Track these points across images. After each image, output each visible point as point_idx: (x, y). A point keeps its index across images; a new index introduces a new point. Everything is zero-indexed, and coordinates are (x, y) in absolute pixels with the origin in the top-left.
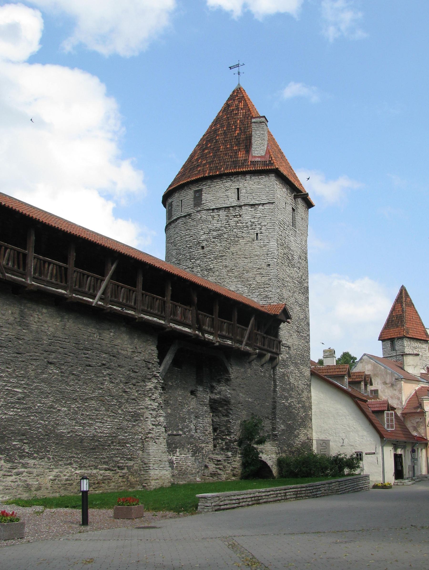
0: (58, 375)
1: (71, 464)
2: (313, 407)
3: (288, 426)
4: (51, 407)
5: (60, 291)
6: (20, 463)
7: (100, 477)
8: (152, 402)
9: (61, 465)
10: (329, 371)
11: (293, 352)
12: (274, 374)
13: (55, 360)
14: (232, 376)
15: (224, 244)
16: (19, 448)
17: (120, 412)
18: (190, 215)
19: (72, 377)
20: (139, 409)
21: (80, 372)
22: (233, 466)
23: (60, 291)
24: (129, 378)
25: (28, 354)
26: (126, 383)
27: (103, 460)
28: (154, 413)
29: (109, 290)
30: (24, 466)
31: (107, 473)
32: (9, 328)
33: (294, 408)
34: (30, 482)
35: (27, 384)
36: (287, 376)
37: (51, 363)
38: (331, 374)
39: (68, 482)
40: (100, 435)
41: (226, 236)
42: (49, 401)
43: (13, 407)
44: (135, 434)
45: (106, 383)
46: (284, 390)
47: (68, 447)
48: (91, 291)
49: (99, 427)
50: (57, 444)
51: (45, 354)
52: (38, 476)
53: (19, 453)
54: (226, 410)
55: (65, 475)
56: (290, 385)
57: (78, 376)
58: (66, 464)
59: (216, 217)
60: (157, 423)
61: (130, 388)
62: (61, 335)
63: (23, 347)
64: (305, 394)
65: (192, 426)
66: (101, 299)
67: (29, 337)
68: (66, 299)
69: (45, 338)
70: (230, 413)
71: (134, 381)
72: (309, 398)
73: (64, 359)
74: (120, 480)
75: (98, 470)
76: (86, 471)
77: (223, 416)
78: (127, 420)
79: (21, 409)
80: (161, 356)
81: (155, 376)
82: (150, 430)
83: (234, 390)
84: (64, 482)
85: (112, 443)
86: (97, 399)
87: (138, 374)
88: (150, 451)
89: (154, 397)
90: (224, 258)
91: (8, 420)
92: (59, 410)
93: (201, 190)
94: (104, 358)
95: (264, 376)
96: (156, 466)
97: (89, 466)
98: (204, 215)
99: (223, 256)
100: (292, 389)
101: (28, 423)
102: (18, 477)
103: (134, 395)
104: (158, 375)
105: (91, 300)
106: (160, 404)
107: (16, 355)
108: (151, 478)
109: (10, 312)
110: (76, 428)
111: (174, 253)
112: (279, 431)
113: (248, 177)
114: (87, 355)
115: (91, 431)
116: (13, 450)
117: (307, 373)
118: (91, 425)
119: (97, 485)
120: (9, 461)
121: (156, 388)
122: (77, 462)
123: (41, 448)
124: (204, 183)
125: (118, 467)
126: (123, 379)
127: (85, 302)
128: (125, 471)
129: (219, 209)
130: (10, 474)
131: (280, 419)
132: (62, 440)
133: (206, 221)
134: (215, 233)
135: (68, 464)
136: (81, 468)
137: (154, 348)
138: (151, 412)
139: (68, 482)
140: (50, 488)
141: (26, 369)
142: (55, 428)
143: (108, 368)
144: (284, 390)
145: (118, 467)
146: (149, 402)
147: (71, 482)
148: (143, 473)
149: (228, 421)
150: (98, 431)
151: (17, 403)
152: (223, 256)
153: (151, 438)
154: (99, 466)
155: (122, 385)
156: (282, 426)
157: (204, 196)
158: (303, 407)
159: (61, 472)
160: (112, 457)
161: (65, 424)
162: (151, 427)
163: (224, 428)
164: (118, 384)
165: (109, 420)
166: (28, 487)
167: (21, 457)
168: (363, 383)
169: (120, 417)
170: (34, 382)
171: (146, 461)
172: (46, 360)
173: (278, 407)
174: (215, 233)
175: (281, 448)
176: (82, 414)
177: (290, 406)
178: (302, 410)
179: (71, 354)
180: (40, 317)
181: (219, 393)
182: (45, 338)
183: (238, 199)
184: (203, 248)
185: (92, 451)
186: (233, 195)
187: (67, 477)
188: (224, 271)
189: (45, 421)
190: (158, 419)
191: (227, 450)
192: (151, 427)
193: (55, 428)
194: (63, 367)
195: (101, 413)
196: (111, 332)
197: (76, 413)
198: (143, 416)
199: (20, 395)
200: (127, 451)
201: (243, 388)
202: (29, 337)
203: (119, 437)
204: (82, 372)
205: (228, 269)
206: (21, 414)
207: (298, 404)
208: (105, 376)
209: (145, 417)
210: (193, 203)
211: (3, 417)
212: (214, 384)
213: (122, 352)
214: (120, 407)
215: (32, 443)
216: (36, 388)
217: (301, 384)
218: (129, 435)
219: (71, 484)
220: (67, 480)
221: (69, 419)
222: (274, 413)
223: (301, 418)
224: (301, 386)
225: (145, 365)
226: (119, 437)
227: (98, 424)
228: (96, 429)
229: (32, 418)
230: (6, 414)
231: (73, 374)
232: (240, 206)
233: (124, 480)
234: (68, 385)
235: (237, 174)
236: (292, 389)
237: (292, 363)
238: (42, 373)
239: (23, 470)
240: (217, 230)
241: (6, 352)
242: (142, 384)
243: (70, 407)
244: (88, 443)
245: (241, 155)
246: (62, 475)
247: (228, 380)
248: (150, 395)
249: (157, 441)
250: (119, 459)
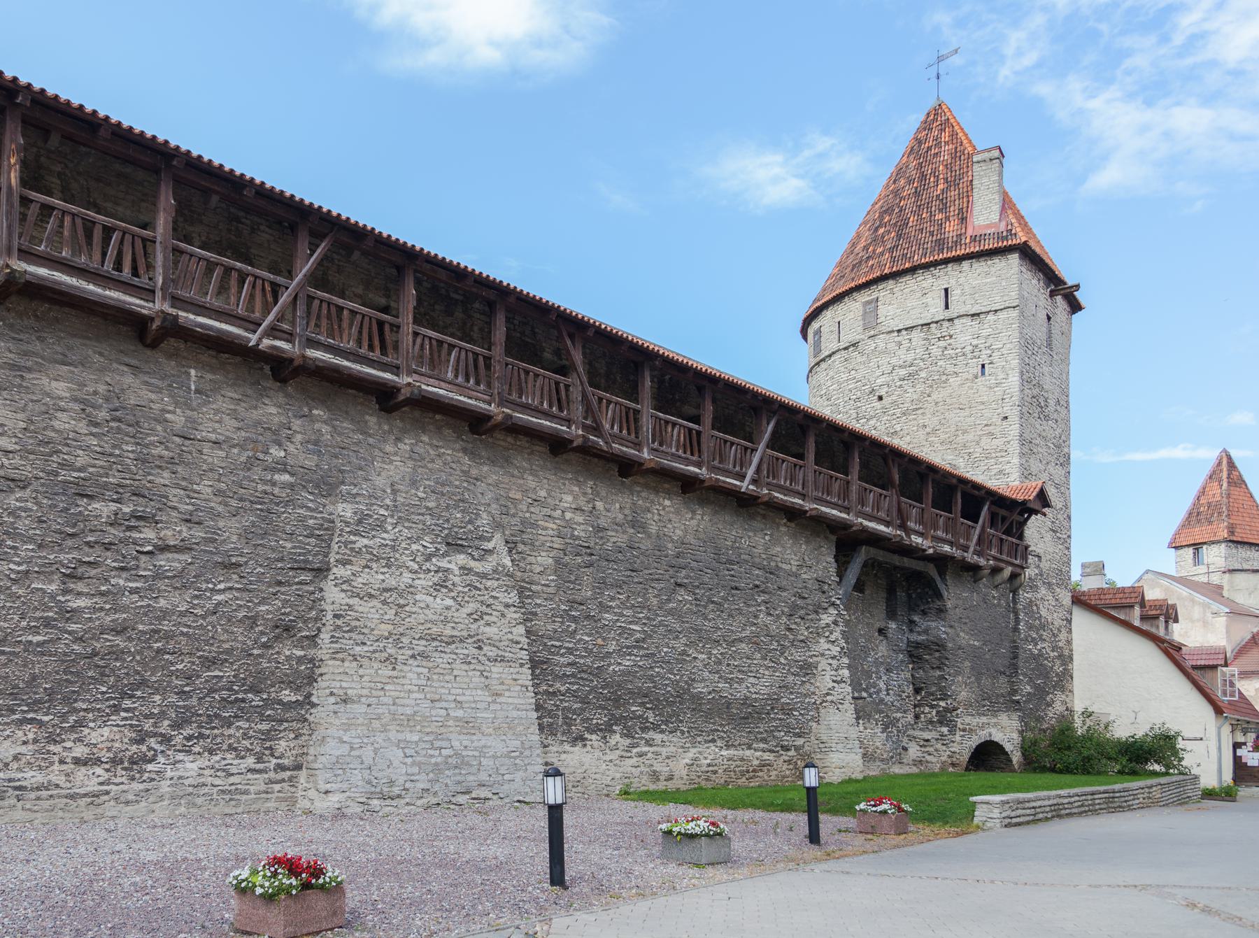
0: (691, 604)
1: (713, 741)
2: (1075, 657)
3: (1036, 687)
4: (684, 653)
5: (692, 468)
6: (642, 738)
7: (756, 762)
8: (830, 646)
9: (699, 743)
10: (1102, 597)
11: (1044, 565)
12: (1015, 601)
13: (686, 581)
14: (949, 604)
16: (641, 716)
17: (782, 660)
19: (711, 606)
20: (811, 657)
21: (722, 598)
22: (952, 749)
23: (692, 468)
24: (794, 607)
25: (647, 572)
26: (791, 615)
27: (759, 736)
28: (834, 662)
29: (765, 466)
30: (649, 743)
31: (766, 756)
32: (617, 531)
33: (1046, 659)
34: (657, 767)
35: (648, 619)
36: (1036, 605)
37: (680, 585)
38: (1107, 602)
39: (711, 769)
40: (754, 696)
41: (923, 374)
42: (679, 645)
43: (630, 654)
44: (806, 696)
45: (762, 616)
46: (1031, 627)
47: (708, 716)
48: (738, 468)
49: (753, 685)
50: (694, 709)
51: (671, 572)
52: (668, 758)
53: (641, 723)
54: (939, 659)
55: (706, 758)
56: (1040, 620)
57: (720, 604)
58: (706, 742)
59: (906, 344)
60: (839, 678)
61: (796, 623)
62: (692, 541)
63: (638, 561)
64: (1063, 636)
65: (882, 685)
66: (754, 481)
67: (646, 545)
68: (703, 481)
69: (670, 545)
70: (946, 665)
71: (802, 612)
72: (1069, 642)
73: (698, 579)
74: (785, 767)
75: (752, 751)
76: (736, 752)
77: (933, 668)
78: (793, 674)
79: (641, 656)
80: (841, 574)
81: (833, 604)
82: (829, 689)
83: (951, 627)
84: (704, 768)
85: (773, 708)
86: (749, 640)
87: (809, 601)
88: (832, 722)
89: (833, 638)
90: (920, 412)
91: (623, 673)
92: (695, 658)
94: (757, 575)
95: (999, 605)
96: (840, 747)
97: (740, 745)
99: (917, 409)
100: (1043, 627)
101: (651, 679)
102: (640, 759)
103: (802, 634)
104: (838, 602)
105: (738, 483)
106: (842, 648)
107: (629, 573)
108: (834, 765)
109: (617, 505)
110: (720, 685)
112: (1024, 696)
114: (732, 572)
115: (741, 691)
116: (632, 718)
117: (1066, 599)
118: (741, 681)
119: (752, 774)
120: (627, 736)
121: (835, 623)
122: (722, 738)
123: (671, 716)
124: (880, 287)
125: (782, 747)
126: (786, 610)
127: (729, 487)
128: (792, 753)
130: (629, 754)
131: (1025, 675)
132: (700, 704)
133: (885, 352)
135: (710, 741)
136: (728, 747)
137: (831, 559)
138: (830, 661)
139: (711, 769)
140: (685, 777)
141: (645, 594)
142: (689, 685)
143: (763, 592)
144: (1031, 627)
145: (782, 747)
146: (826, 646)
147: (716, 768)
148: (819, 756)
149: (942, 677)
150: (752, 690)
151: (635, 647)
152: (917, 409)
153: (832, 702)
154: (754, 745)
155: (784, 620)
156: (1028, 687)
157: (882, 310)
158: (1060, 656)
159: (700, 753)
160: (772, 731)
161: (703, 680)
162: (831, 684)
163: (934, 689)
164: (778, 617)
165: (767, 673)
166: (655, 776)
167: (644, 729)
168: (1162, 619)
169: (784, 669)
170: (657, 615)
171: (824, 738)
172: (672, 581)
173: (1022, 655)
174: (903, 372)
175: (1026, 723)
176: (728, 665)
177: (1041, 655)
178: (1058, 662)
179: (709, 571)
180: (661, 512)
181: (926, 632)
182: (670, 545)
185: (743, 721)
187: (708, 761)
188: (922, 433)
189: (675, 675)
190: (840, 672)
191: (941, 723)
192: (831, 684)
193: (689, 685)
194: (698, 591)
195: (755, 662)
196: (766, 534)
197: (719, 663)
198: (816, 668)
199: (638, 635)
200: (794, 722)
201: (966, 623)
202: (646, 545)
203: (782, 700)
204: (725, 599)
205: (928, 430)
206: (641, 663)
207: (1053, 651)
208: (759, 605)
209: (820, 669)
210: (861, 323)
211: (617, 669)
212: (916, 618)
213: (784, 566)
214: (782, 654)
215: (658, 709)
216: (661, 624)
217: (1056, 619)
218: (797, 697)
219: (715, 772)
220: (709, 765)
221: (710, 672)
222: (1015, 667)
223: (1057, 675)
224: (1058, 623)
225: (817, 587)
226: (782, 700)
227: (752, 680)
228: (748, 687)
229: (657, 670)
230: (620, 664)
231: (713, 602)
233: (791, 767)
234: (706, 618)
236: (1043, 627)
237: (1044, 583)
238: (669, 600)
239: (646, 749)
240: (906, 367)
241: (615, 569)
242: (813, 616)
243: (710, 653)
244: (738, 709)
246: (701, 757)
247: (941, 611)
248: (827, 634)
249: (840, 706)
250: (782, 734)
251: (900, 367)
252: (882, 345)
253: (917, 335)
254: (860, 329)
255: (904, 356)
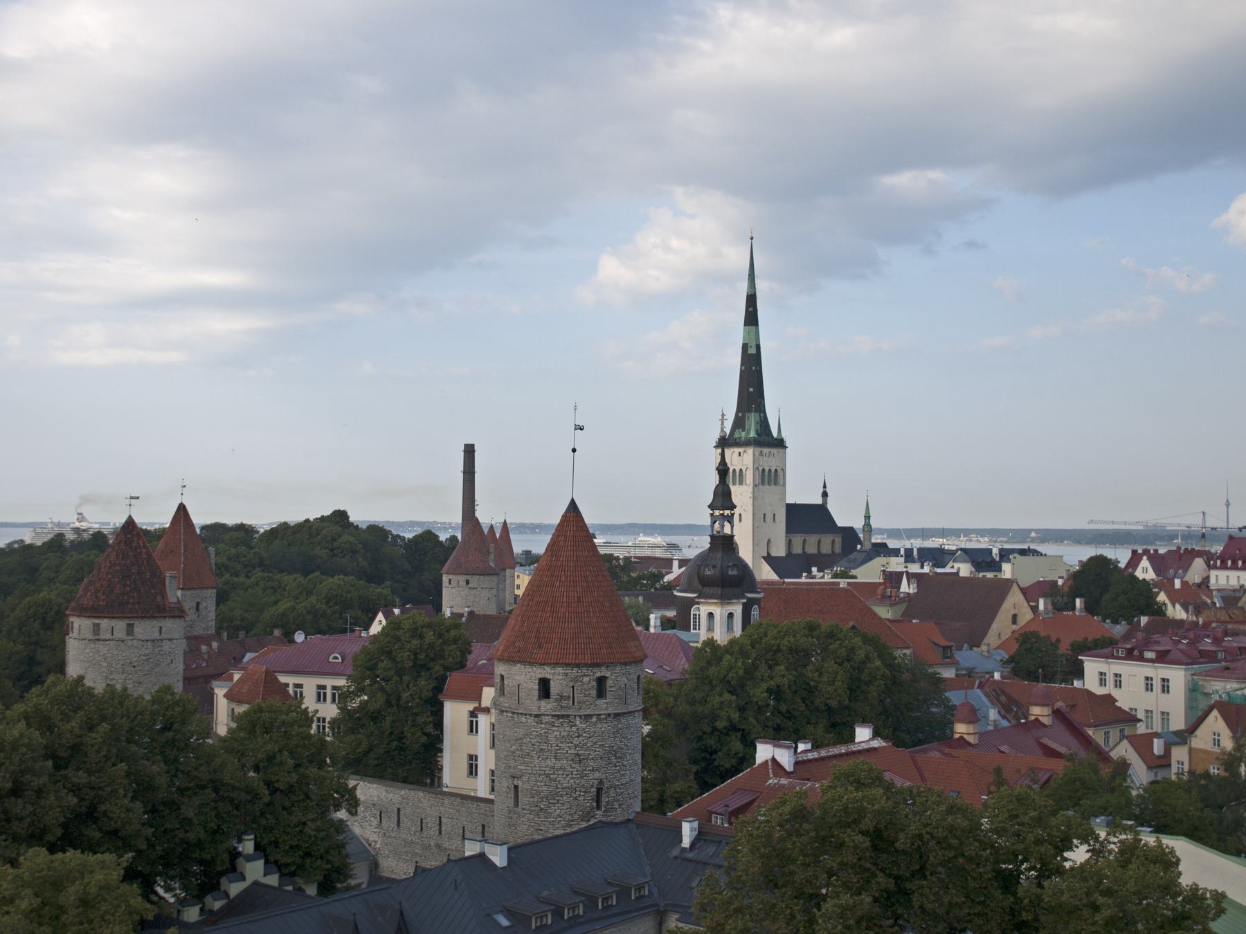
15: (150, 665)
18: (123, 641)
93: (133, 624)
98: (135, 643)
111: (105, 664)
113: (167, 619)
129: (147, 641)
134: (144, 658)
174: (144, 658)
183: (160, 634)
184: (134, 667)
186: (156, 630)
232: (162, 640)
235: (161, 617)
245: (159, 598)
251: (144, 655)
252: (135, 645)
253: (149, 643)
254: (125, 634)
255: (143, 651)
